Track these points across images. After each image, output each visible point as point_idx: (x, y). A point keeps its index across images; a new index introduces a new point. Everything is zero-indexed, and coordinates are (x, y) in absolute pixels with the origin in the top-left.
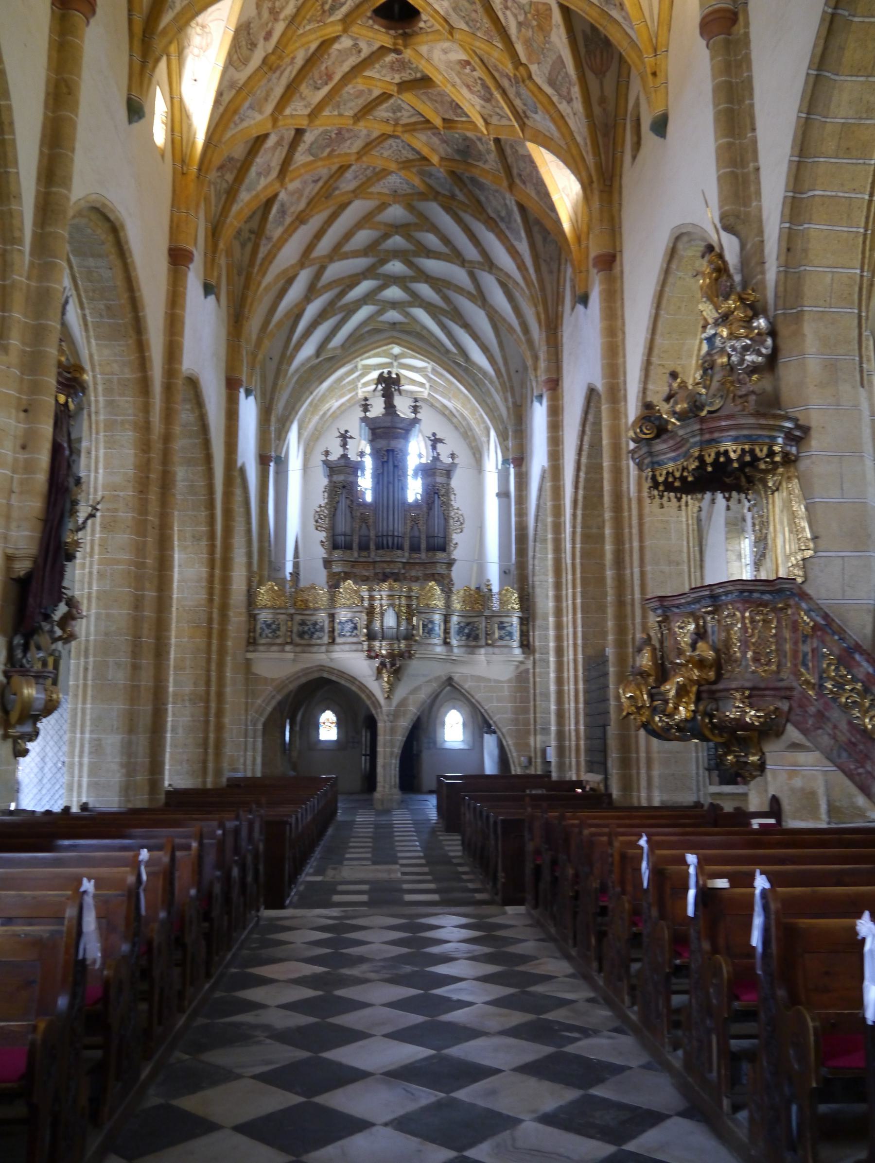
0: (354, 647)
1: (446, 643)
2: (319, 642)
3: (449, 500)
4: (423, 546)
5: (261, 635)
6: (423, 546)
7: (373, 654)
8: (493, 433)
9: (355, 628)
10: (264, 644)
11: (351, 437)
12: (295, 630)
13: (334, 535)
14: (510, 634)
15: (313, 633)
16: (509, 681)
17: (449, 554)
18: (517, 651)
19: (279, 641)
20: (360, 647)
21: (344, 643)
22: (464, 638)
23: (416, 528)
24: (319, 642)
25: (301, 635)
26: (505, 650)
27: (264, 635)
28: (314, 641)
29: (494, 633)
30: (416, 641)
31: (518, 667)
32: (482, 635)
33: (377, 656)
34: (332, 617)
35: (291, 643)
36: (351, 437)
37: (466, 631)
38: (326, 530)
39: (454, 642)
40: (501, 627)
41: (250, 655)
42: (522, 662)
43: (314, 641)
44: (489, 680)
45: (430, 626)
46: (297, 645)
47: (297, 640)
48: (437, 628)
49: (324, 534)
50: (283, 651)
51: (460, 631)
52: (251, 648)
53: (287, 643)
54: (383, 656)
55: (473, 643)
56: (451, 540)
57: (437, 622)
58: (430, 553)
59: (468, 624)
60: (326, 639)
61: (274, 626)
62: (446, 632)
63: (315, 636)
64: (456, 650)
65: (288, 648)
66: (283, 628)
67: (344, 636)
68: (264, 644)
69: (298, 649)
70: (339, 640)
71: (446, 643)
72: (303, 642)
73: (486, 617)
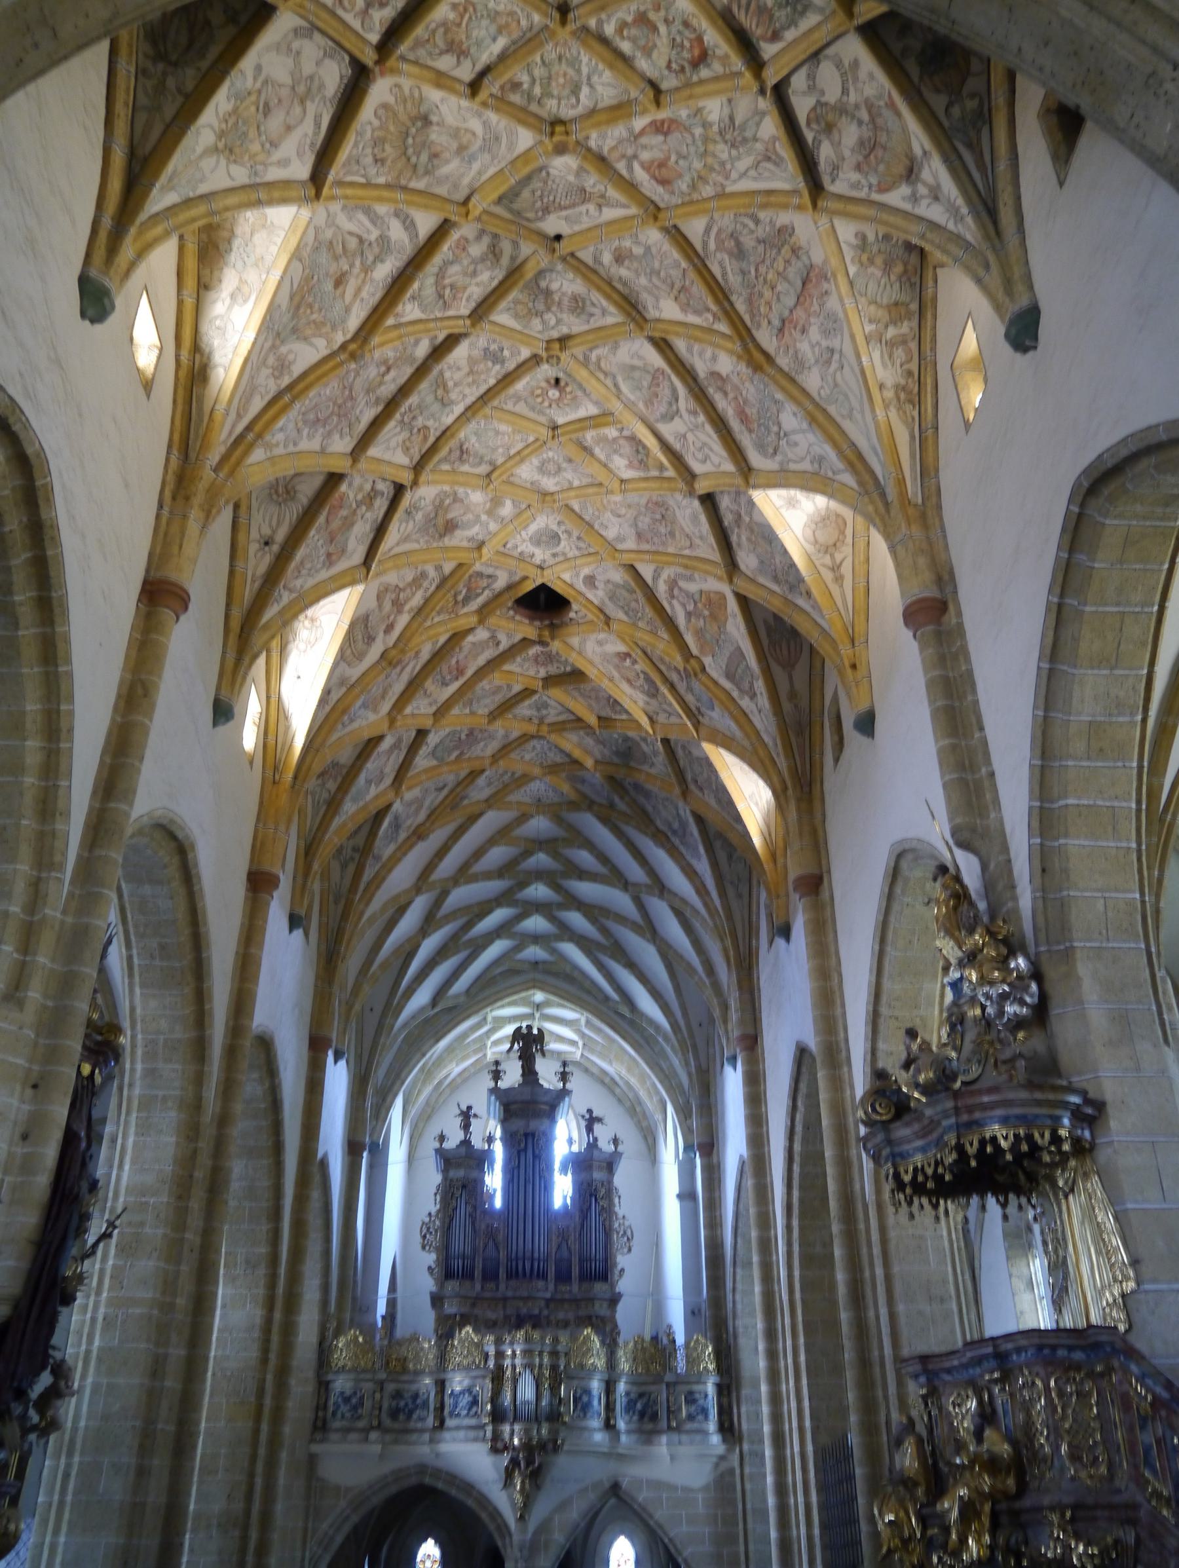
0: (472, 1434)
1: (609, 1426)
2: (419, 1425)
3: (611, 1204)
4: (575, 1272)
5: (334, 1413)
6: (575, 1272)
7: (500, 1445)
8: (670, 1109)
9: (474, 1402)
10: (337, 1430)
11: (475, 1116)
12: (385, 1405)
13: (447, 1258)
14: (704, 1411)
15: (411, 1413)
16: (706, 1488)
17: (613, 1286)
18: (715, 1439)
19: (361, 1424)
20: (481, 1434)
21: (458, 1428)
22: (635, 1418)
23: (564, 1246)
24: (419, 1425)
25: (394, 1414)
26: (698, 1437)
27: (339, 1415)
28: (412, 1425)
29: (680, 1409)
30: (564, 1423)
31: (717, 1465)
32: (663, 1414)
33: (506, 1448)
34: (441, 1385)
35: (379, 1426)
36: (475, 1116)
37: (639, 1406)
38: (437, 1249)
39: (621, 1425)
40: (691, 1399)
41: (315, 1448)
42: (722, 1458)
43: (412, 1425)
44: (674, 1488)
45: (585, 1399)
46: (386, 1431)
47: (387, 1422)
48: (595, 1403)
49: (433, 1256)
50: (366, 1440)
51: (630, 1406)
52: (318, 1436)
53: (372, 1428)
54: (514, 1448)
55: (650, 1426)
56: (615, 1264)
57: (595, 1392)
58: (585, 1285)
59: (641, 1395)
60: (430, 1421)
61: (354, 1401)
62: (610, 1408)
63: (415, 1416)
64: (624, 1438)
65: (374, 1435)
66: (368, 1404)
67: (458, 1415)
68: (337, 1430)
69: (388, 1437)
70: (450, 1423)
71: (609, 1426)
72: (396, 1426)
73: (668, 1385)
